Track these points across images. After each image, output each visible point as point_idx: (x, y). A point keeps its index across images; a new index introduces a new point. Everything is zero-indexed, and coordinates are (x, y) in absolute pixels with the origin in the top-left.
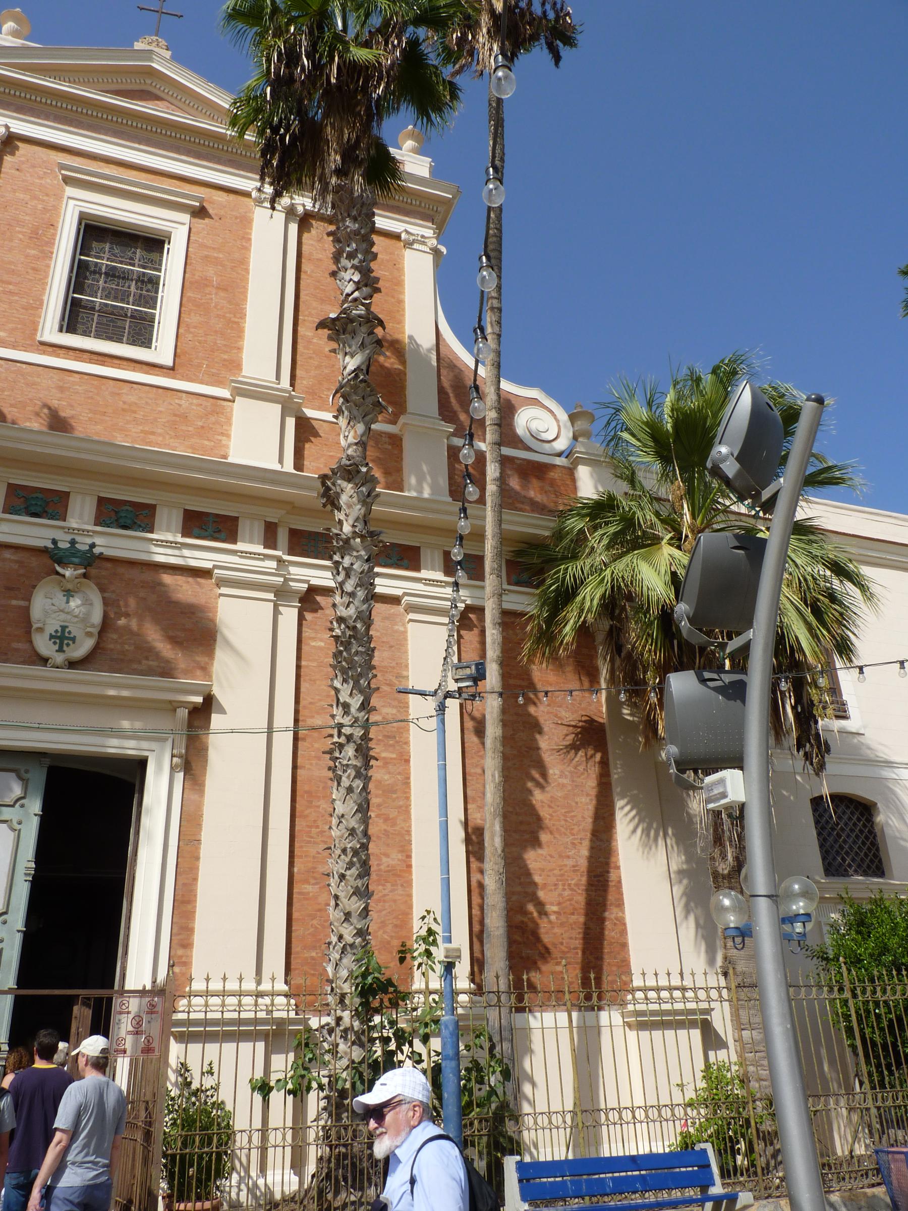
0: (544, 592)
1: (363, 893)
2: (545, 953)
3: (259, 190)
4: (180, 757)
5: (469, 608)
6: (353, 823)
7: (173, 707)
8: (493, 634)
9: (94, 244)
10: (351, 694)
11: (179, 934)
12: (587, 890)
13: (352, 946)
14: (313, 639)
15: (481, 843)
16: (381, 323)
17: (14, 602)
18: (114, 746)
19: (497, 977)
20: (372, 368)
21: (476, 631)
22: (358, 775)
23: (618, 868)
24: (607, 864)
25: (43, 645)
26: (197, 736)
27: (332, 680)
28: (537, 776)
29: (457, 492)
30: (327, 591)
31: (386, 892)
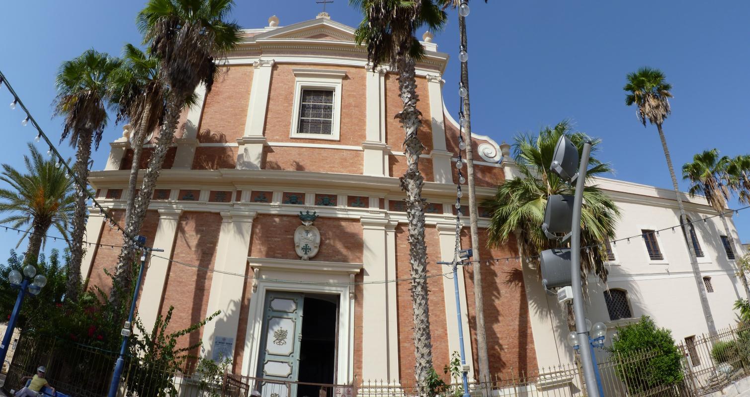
0: (494, 219)
1: (428, 346)
2: (504, 365)
3: (368, 65)
4: (353, 293)
5: (464, 228)
6: (422, 318)
7: (349, 274)
8: (474, 238)
9: (307, 97)
10: (418, 266)
11: (356, 363)
12: (519, 338)
13: (425, 367)
14: (402, 244)
15: (475, 323)
16: (420, 113)
17: (288, 236)
18: (328, 290)
19: (485, 376)
20: (418, 132)
21: (467, 237)
22: (423, 298)
23: (531, 328)
24: (527, 327)
25: (300, 252)
26: (359, 285)
27: (410, 260)
28: (496, 294)
29: (456, 180)
30: (406, 224)
31: (437, 345)
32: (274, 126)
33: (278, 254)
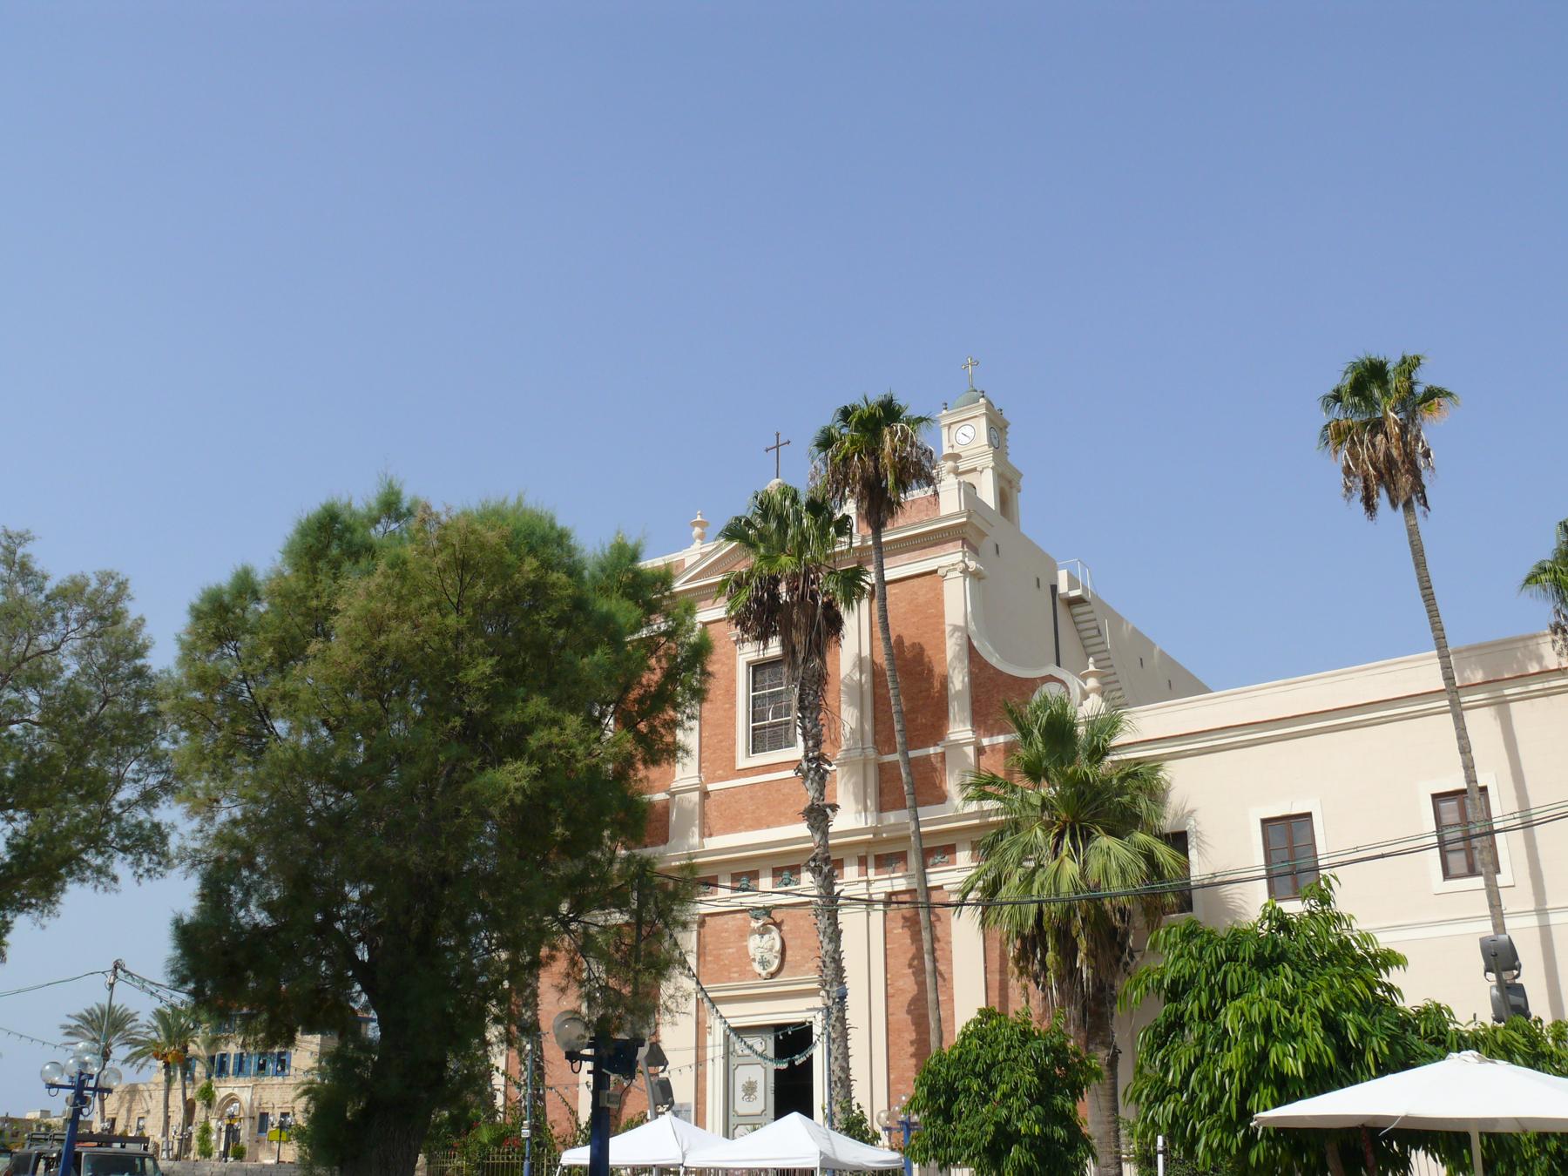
14: (894, 928)
32: (714, 752)
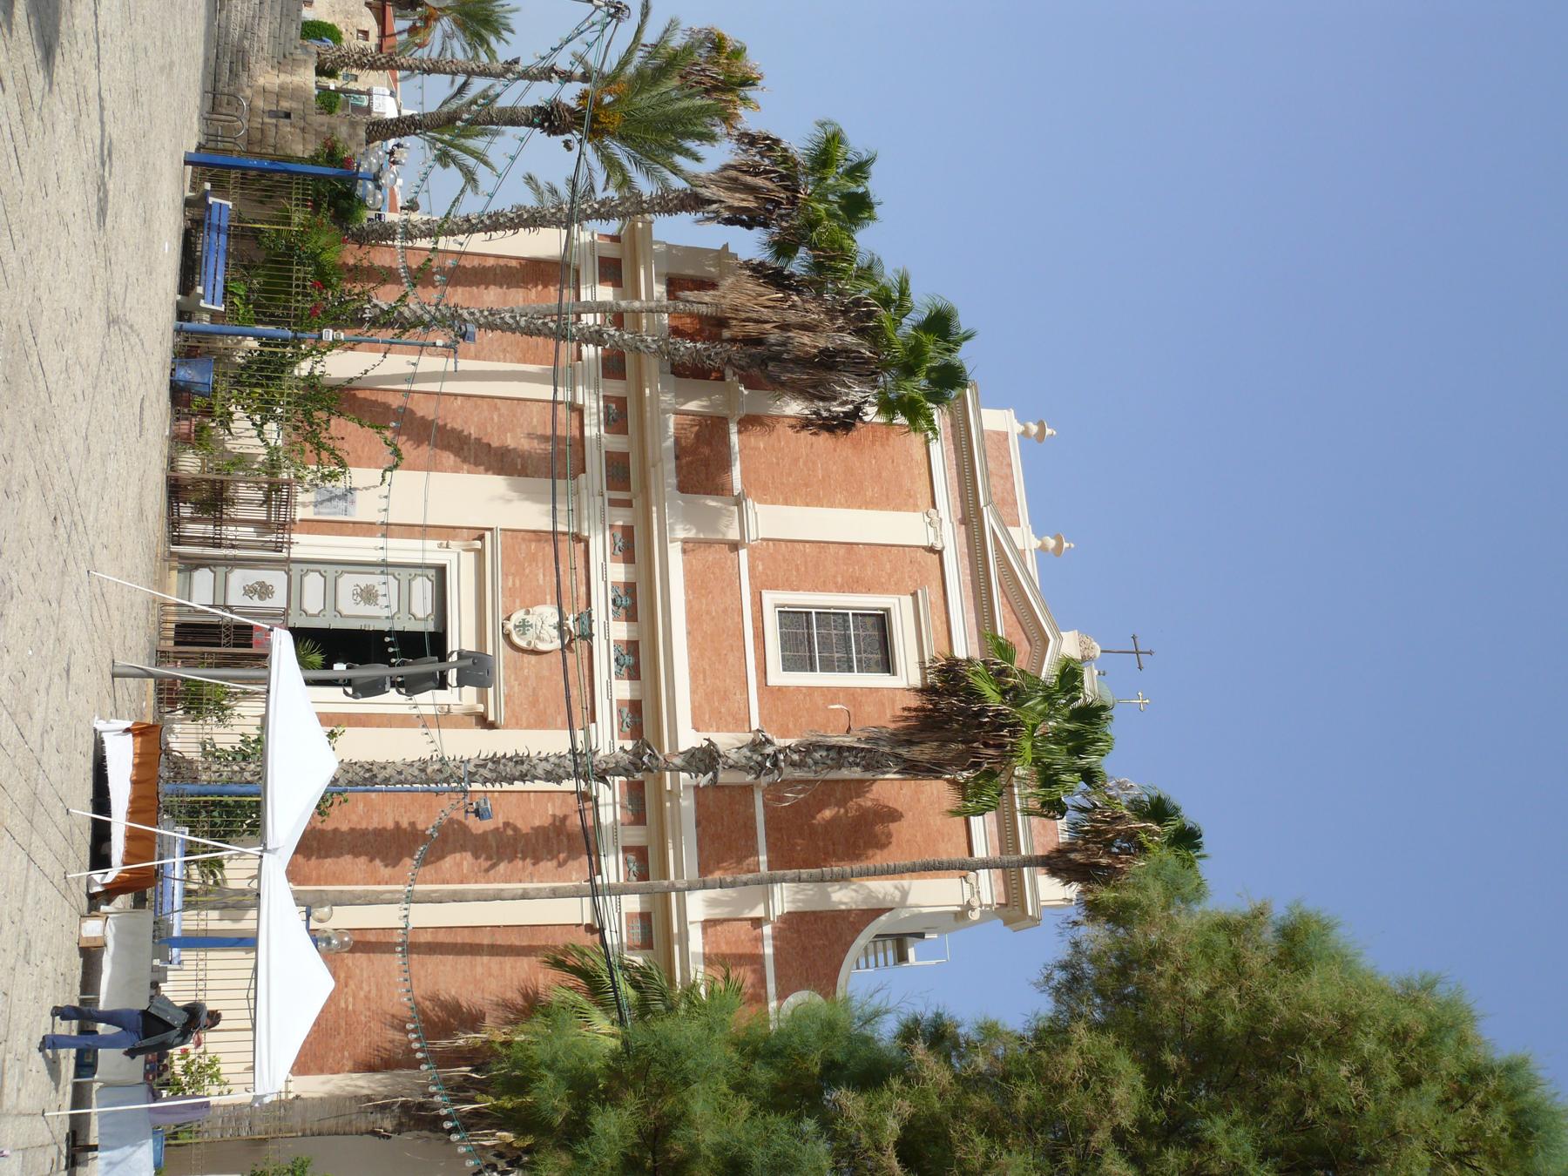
14: (554, 805)
25: (518, 616)
33: (514, 581)
